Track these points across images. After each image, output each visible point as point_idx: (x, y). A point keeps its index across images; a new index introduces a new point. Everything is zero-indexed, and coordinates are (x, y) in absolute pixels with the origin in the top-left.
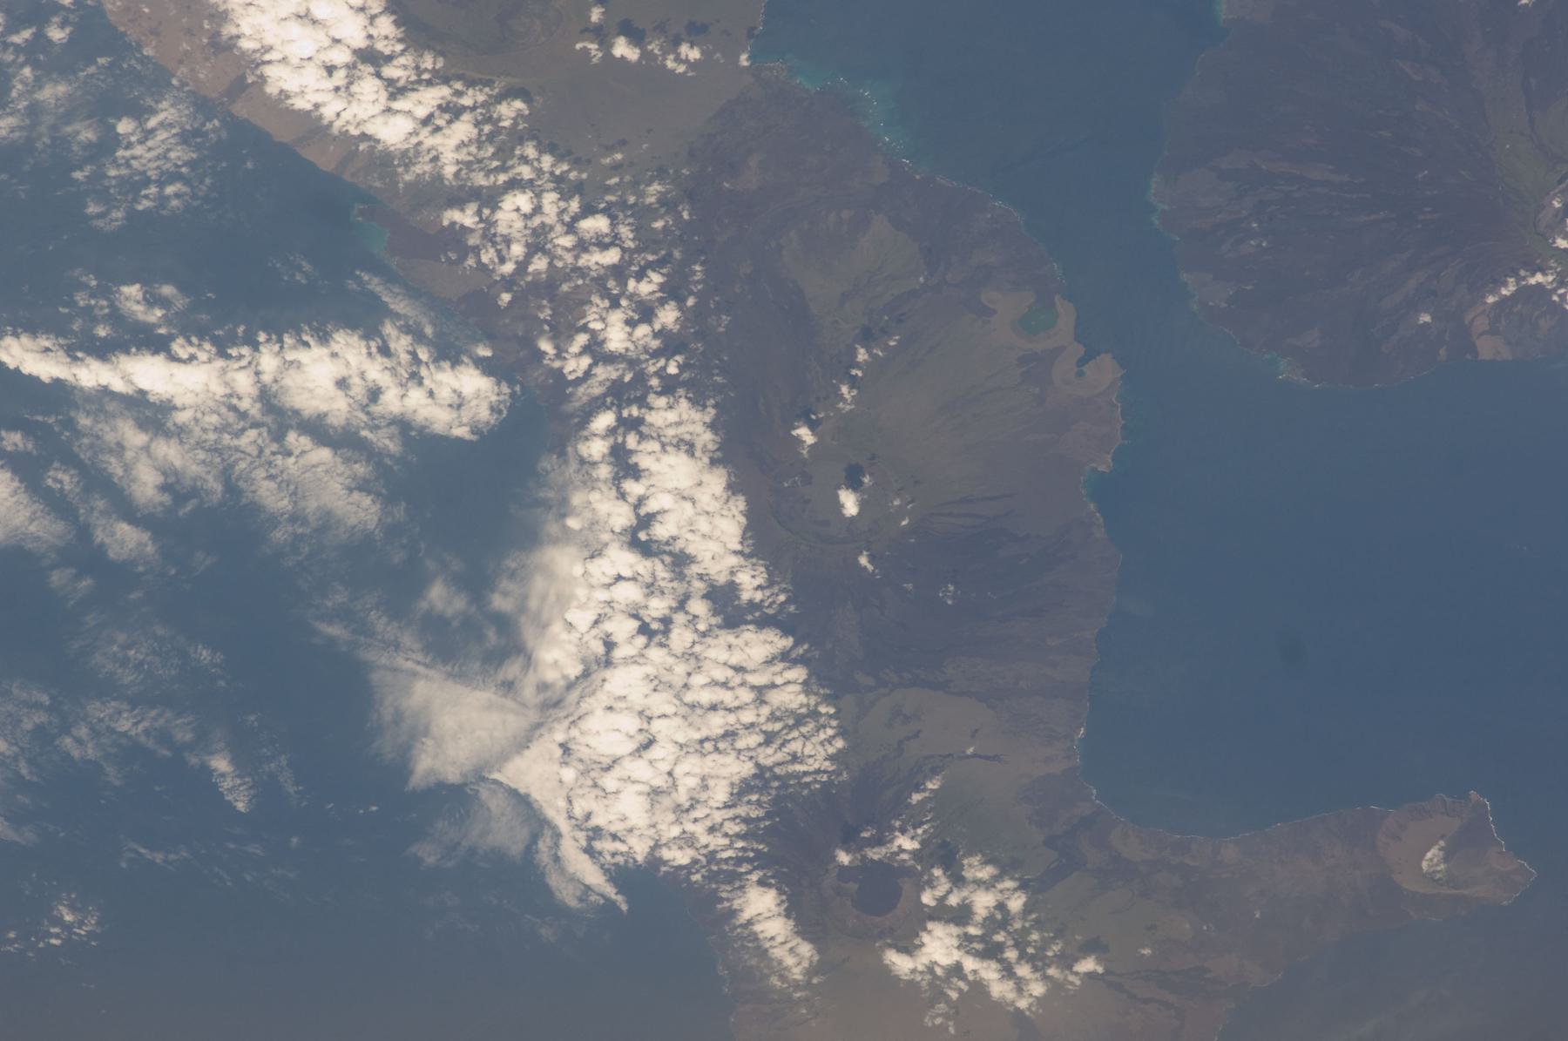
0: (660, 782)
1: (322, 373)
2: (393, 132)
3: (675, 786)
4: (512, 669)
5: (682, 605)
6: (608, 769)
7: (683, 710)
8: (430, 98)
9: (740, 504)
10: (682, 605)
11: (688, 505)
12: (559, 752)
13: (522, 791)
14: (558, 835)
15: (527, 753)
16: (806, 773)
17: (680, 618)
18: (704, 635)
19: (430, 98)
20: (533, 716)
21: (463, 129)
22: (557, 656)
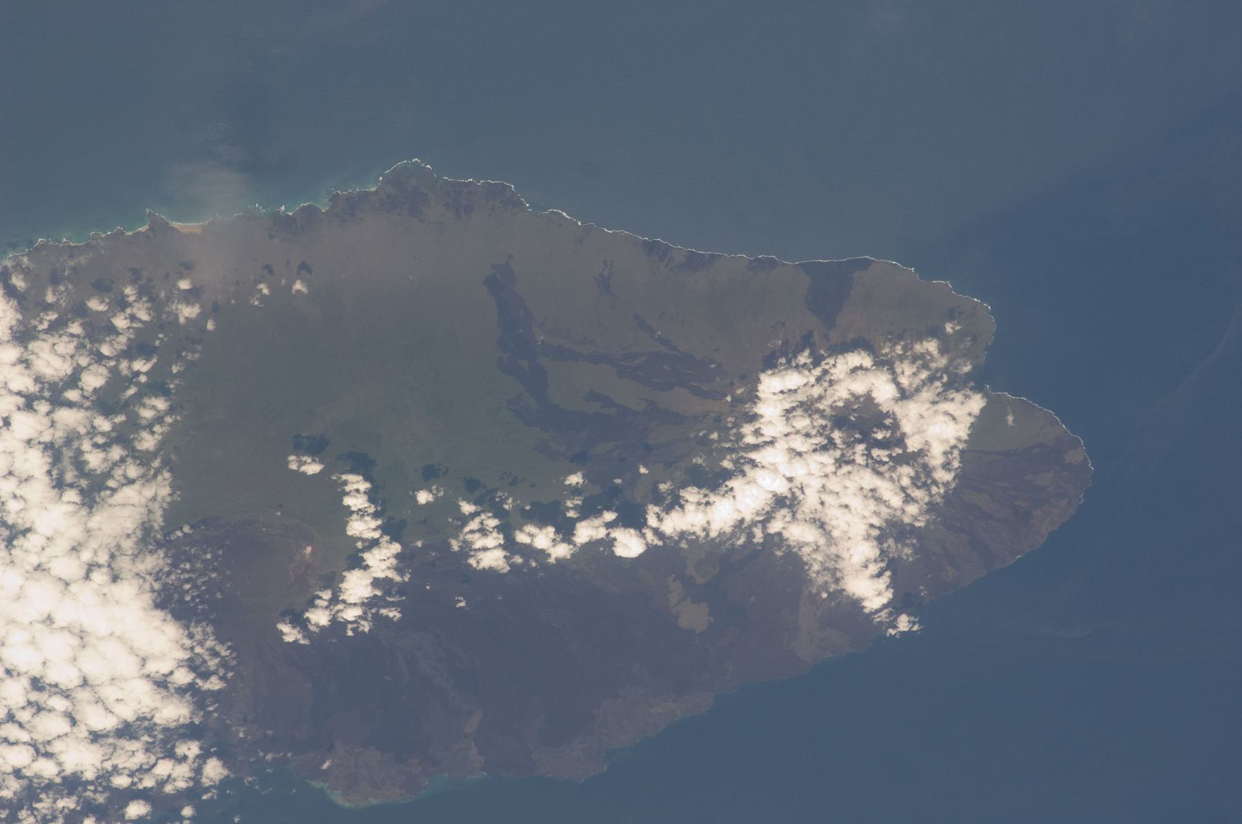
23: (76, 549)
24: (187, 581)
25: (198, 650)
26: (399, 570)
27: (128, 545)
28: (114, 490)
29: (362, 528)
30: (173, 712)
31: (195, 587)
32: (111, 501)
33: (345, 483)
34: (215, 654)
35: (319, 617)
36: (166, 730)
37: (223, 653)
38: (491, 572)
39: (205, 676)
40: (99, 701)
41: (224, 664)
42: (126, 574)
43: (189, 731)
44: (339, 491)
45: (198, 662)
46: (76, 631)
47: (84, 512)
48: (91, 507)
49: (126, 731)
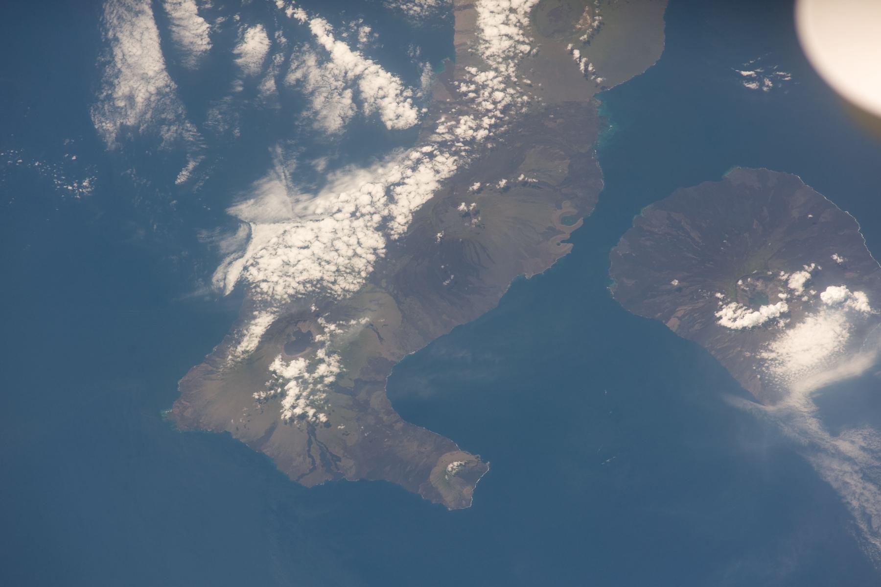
0: (293, 261)
1: (380, 83)
3: (294, 265)
4: (304, 197)
5: (372, 214)
6: (286, 247)
7: (329, 244)
9: (430, 196)
10: (372, 214)
11: (416, 187)
12: (281, 231)
13: (253, 236)
14: (242, 257)
15: (272, 225)
16: (331, 289)
17: (367, 217)
18: (367, 226)
20: (290, 216)
22: (322, 203)
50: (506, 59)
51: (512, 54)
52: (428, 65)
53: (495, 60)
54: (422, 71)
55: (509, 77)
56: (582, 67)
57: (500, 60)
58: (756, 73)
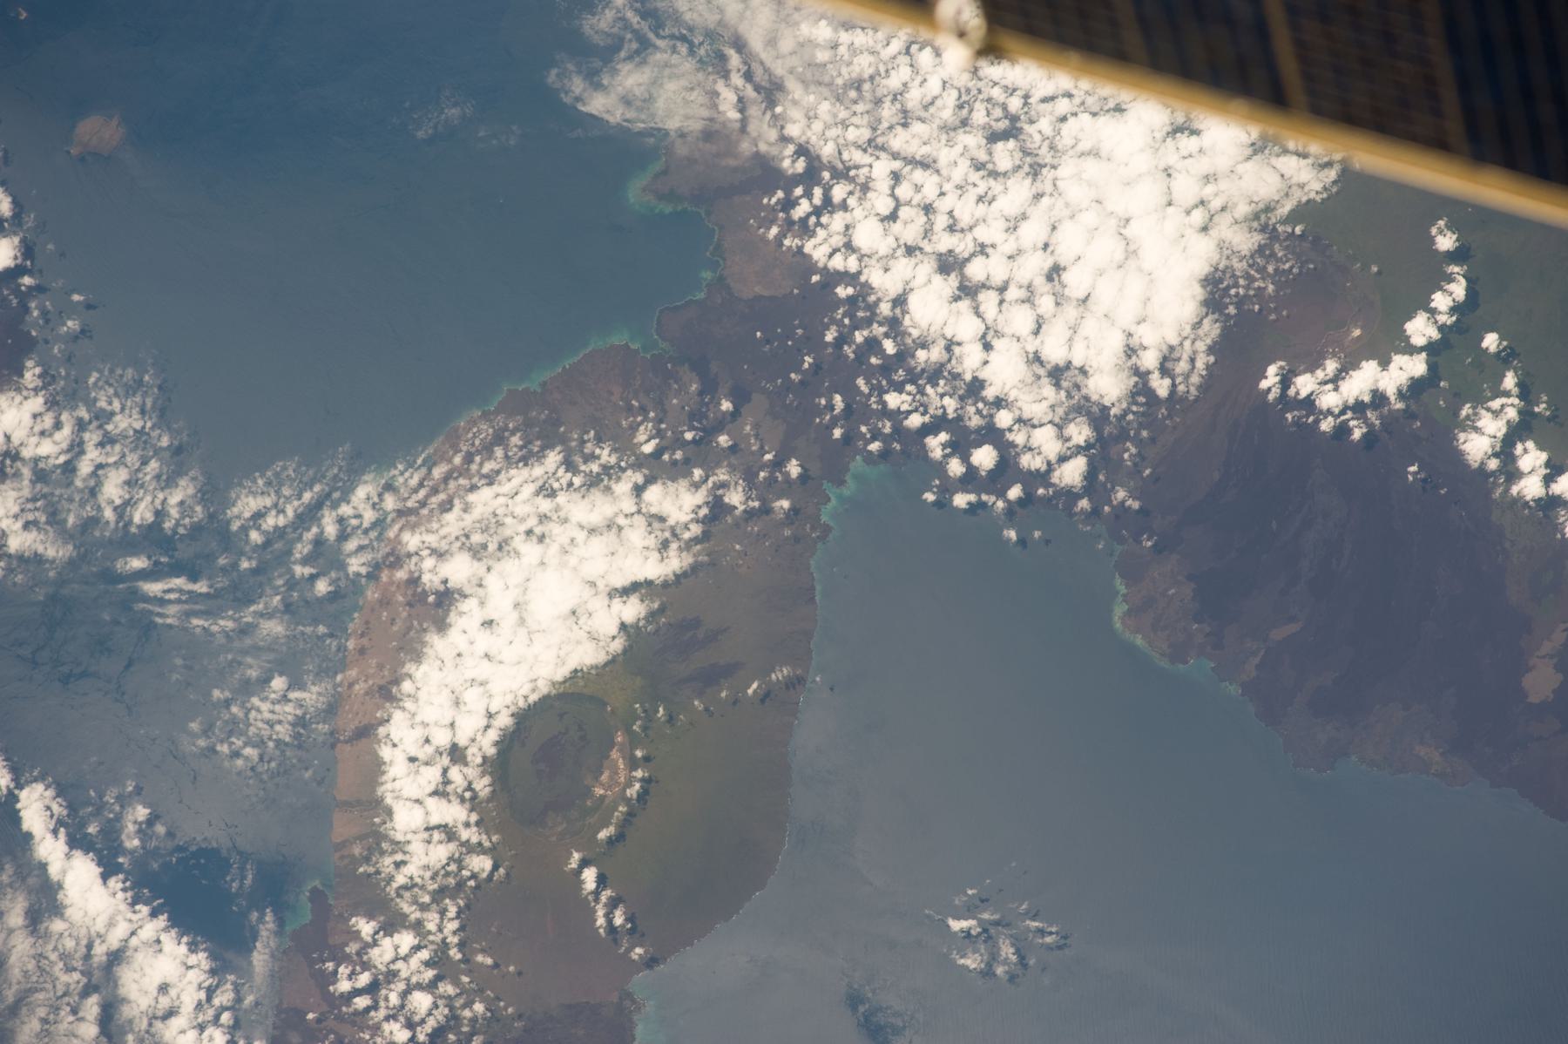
2: (405, 820)
8: (453, 813)
19: (453, 813)
21: (440, 853)
23: (1208, 179)
24: (1248, 277)
25: (1187, 344)
26: (1400, 394)
27: (1243, 210)
28: (1286, 151)
29: (1420, 329)
30: (1108, 387)
31: (1247, 287)
32: (1274, 161)
33: (1450, 279)
34: (1192, 360)
35: (1304, 384)
36: (1087, 399)
37: (1200, 364)
38: (1458, 456)
39: (1164, 371)
40: (1074, 329)
41: (1187, 376)
42: (1213, 233)
43: (1097, 415)
44: (1439, 280)
45: (1176, 355)
46: (1132, 247)
47: (1249, 151)
48: (1255, 153)
49: (1057, 374)
50: (439, 895)
51: (452, 881)
52: (269, 917)
53: (415, 902)
54: (255, 938)
55: (444, 944)
56: (601, 921)
57: (427, 899)
58: (981, 922)
